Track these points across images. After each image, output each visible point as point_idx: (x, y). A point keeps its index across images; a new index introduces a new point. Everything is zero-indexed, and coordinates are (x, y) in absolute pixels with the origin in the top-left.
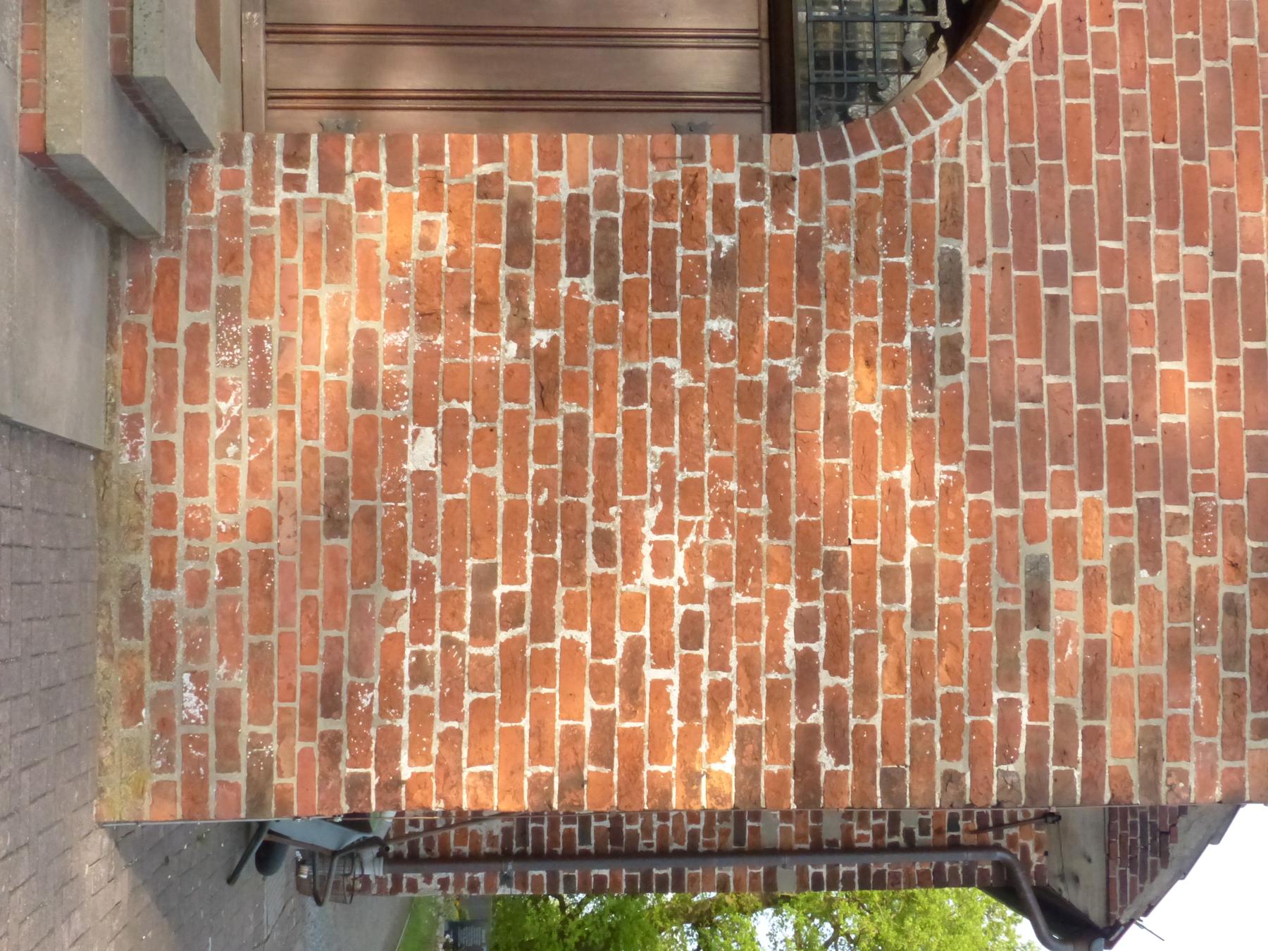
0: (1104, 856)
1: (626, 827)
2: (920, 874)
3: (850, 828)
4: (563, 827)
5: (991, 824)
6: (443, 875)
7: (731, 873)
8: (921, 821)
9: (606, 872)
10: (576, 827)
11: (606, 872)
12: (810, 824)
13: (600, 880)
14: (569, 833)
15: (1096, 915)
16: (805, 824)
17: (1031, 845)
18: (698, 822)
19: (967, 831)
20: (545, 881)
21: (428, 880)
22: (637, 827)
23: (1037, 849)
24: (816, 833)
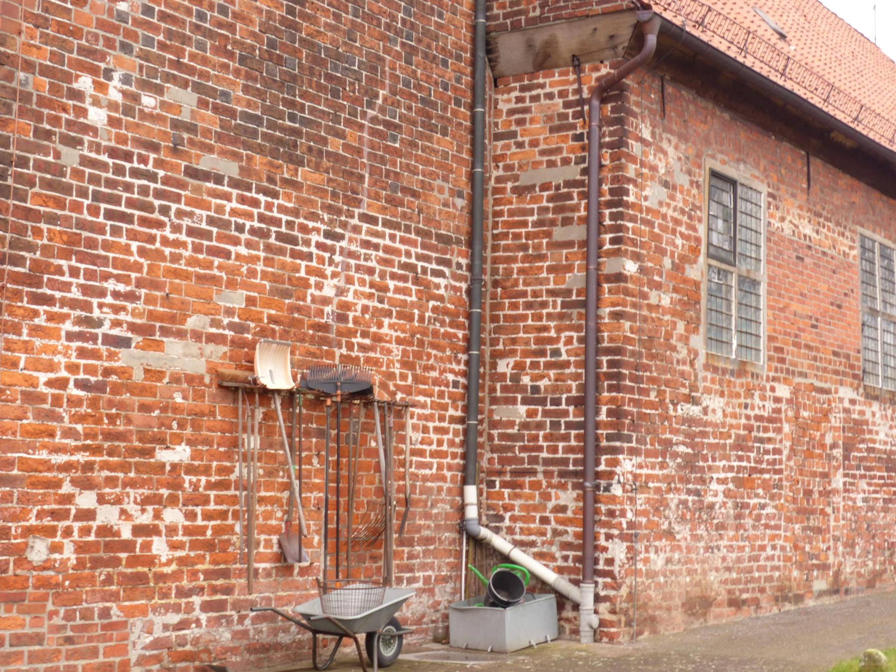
0: (589, 19)
1: (574, 393)
2: (612, 160)
3: (579, 218)
4: (573, 443)
5: (579, 108)
6: (602, 537)
7: (608, 310)
8: (576, 163)
9: (604, 409)
10: (573, 433)
11: (604, 409)
12: (576, 249)
13: (610, 413)
14: (577, 437)
15: (629, 20)
16: (575, 253)
17: (595, 75)
18: (572, 338)
19: (583, 127)
20: (609, 456)
21: (605, 549)
22: (574, 385)
23: (597, 69)
24: (585, 244)
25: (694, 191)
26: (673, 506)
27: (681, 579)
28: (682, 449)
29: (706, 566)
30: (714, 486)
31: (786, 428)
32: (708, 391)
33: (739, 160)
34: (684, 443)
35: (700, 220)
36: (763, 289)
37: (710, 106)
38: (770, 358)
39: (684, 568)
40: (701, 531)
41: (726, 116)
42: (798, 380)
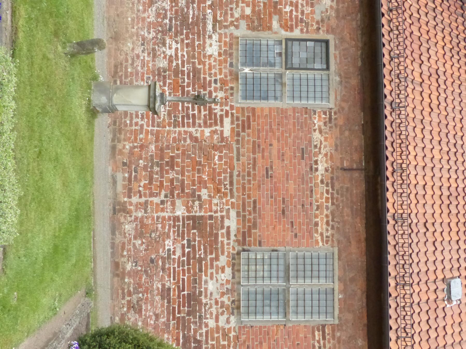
25: (315, 27)
26: (164, 4)
27: (129, 13)
28: (191, 12)
29: (135, 38)
30: (174, 46)
31: (207, 132)
32: (220, 41)
33: (340, 76)
34: (194, 14)
35: (302, 30)
36: (277, 104)
37: (360, 45)
38: (243, 109)
39: (135, 16)
40: (152, 35)
41: (360, 64)
42: (235, 146)
